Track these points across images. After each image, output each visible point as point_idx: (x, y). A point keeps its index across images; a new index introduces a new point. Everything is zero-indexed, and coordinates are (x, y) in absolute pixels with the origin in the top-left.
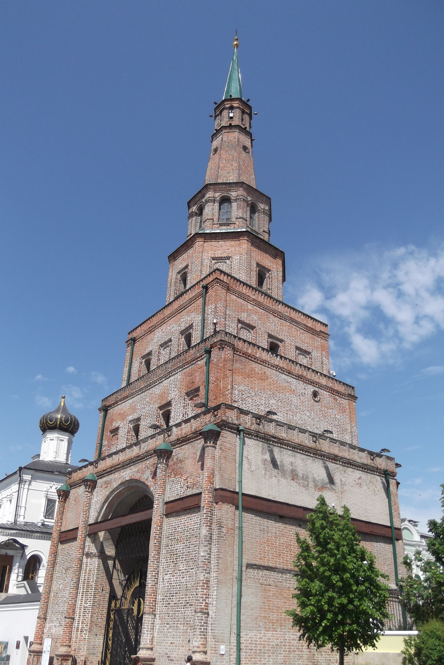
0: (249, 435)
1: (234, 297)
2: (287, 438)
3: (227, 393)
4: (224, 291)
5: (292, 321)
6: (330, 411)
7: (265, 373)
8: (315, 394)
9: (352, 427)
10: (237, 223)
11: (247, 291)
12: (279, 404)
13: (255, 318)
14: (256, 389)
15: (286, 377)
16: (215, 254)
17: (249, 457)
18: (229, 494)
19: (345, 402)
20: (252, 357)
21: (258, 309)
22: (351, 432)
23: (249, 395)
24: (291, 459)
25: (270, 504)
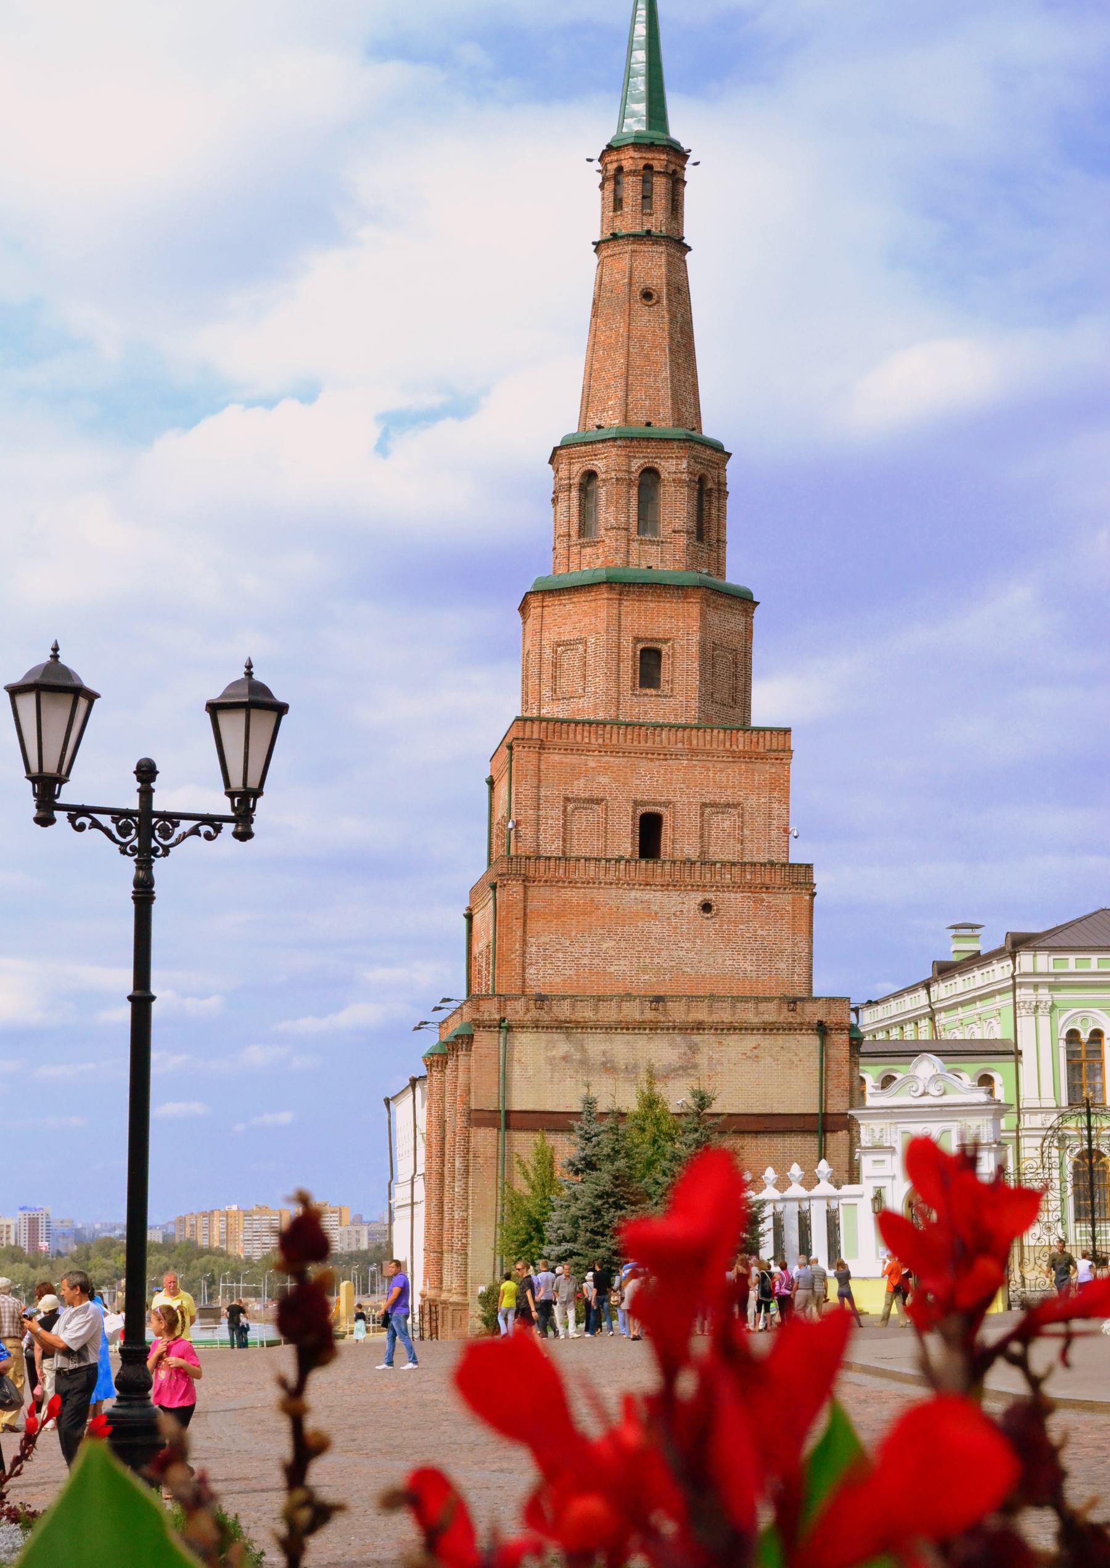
0: (523, 1027)
1: (556, 758)
2: (594, 1018)
3: (513, 956)
4: (533, 757)
5: (694, 752)
6: (742, 927)
7: (592, 900)
8: (706, 907)
9: (795, 945)
10: (607, 541)
11: (586, 734)
12: (623, 944)
13: (604, 780)
14: (573, 934)
15: (639, 894)
16: (559, 633)
17: (523, 1060)
18: (487, 1115)
19: (784, 900)
20: (564, 882)
21: (612, 759)
22: (793, 954)
23: (558, 947)
24: (603, 1047)
25: (555, 1117)
